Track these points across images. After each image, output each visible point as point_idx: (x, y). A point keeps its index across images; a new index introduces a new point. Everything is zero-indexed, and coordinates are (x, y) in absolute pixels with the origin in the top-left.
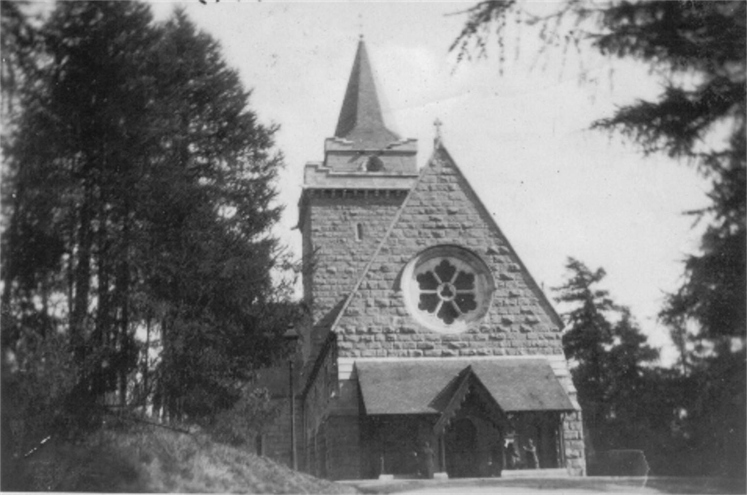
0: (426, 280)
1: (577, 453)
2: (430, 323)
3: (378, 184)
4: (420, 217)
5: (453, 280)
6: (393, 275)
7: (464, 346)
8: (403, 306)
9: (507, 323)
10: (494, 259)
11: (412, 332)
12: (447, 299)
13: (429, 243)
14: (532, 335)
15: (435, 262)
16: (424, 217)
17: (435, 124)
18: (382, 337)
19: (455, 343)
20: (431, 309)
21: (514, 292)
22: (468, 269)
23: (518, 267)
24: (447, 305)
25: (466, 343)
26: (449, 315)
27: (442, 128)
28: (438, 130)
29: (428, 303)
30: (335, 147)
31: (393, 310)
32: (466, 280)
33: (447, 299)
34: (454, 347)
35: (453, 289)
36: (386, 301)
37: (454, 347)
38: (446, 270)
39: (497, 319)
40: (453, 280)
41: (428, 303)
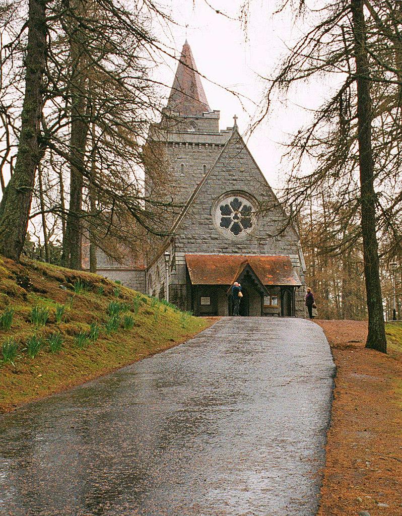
0: (225, 210)
2: (228, 233)
4: (223, 173)
11: (216, 239)
12: (236, 221)
15: (231, 199)
17: (234, 118)
19: (239, 246)
24: (236, 225)
26: (236, 230)
28: (235, 121)
29: (225, 223)
31: (207, 226)
34: (239, 248)
35: (239, 215)
37: (239, 248)
38: (236, 204)
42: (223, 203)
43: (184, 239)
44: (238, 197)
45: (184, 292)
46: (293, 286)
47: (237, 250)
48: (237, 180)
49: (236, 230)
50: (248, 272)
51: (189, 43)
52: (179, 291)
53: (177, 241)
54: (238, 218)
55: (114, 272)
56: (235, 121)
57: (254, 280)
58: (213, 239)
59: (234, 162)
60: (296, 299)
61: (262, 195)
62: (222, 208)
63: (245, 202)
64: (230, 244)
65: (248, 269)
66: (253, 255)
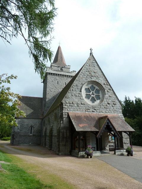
0: (87, 90)
1: (128, 143)
2: (88, 102)
3: (62, 73)
4: (86, 73)
7: (98, 110)
8: (82, 97)
9: (109, 104)
12: (93, 96)
13: (89, 80)
15: (90, 85)
16: (88, 73)
17: (90, 50)
18: (76, 105)
19: (95, 108)
20: (89, 98)
21: (110, 96)
22: (98, 88)
26: (93, 100)
27: (92, 51)
29: (88, 96)
30: (54, 65)
31: (79, 98)
33: (93, 96)
34: (95, 110)
36: (77, 95)
37: (95, 110)
39: (106, 103)
43: (67, 103)
44: (93, 85)
45: (68, 134)
47: (94, 111)
48: (93, 76)
49: (93, 100)
50: (108, 123)
51: (60, 46)
52: (65, 134)
54: (94, 95)
55: (30, 119)
57: (111, 128)
61: (104, 84)
63: (97, 87)
64: (91, 107)
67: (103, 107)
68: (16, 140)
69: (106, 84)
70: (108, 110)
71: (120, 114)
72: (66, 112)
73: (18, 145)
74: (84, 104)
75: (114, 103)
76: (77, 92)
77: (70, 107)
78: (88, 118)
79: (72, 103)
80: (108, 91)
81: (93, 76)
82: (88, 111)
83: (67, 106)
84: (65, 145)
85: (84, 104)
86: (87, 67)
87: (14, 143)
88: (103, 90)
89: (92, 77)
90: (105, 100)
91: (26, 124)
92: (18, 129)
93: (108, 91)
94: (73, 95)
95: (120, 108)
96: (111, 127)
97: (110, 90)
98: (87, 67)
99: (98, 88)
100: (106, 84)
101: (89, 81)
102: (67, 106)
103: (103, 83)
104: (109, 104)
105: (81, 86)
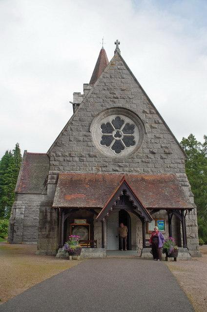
0: (106, 128)
1: (194, 236)
2: (108, 152)
4: (104, 92)
5: (122, 128)
6: (86, 123)
7: (126, 166)
8: (91, 141)
9: (153, 153)
10: (146, 116)
14: (168, 161)
15: (111, 118)
16: (107, 93)
18: (77, 159)
19: (120, 164)
20: (108, 145)
21: (157, 135)
22: (131, 122)
23: (160, 121)
24: (118, 142)
25: (127, 164)
26: (118, 148)
29: (106, 141)
30: (88, 87)
31: (85, 143)
32: (129, 128)
33: (118, 138)
34: (120, 166)
35: (122, 133)
36: (81, 138)
37: (120, 166)
38: (119, 122)
39: (147, 151)
40: (122, 128)
41: (106, 141)
42: (105, 121)
43: (59, 156)
46: (183, 210)
47: (118, 168)
48: (117, 98)
49: (118, 148)
50: (124, 191)
51: (105, 48)
52: (49, 214)
53: (52, 158)
54: (120, 136)
56: (117, 48)
58: (90, 156)
59: (116, 82)
60: (187, 224)
61: (144, 112)
62: (103, 126)
63: (127, 120)
65: (125, 188)
66: (136, 171)
67: (139, 160)
68: (18, 233)
69: (148, 112)
70: (150, 165)
71: (178, 175)
72: (54, 174)
73: (21, 243)
74: (95, 156)
75: (166, 150)
76: (81, 133)
77: (65, 164)
78: (94, 182)
79: (70, 154)
80: (152, 127)
81: (117, 98)
82: (104, 169)
83: (58, 161)
84: (48, 237)
85: (95, 156)
86: (105, 80)
87: (14, 240)
88: (141, 123)
89: (115, 100)
90: (145, 146)
91: (35, 204)
92: (21, 214)
93: (152, 127)
94: (72, 139)
95: (180, 161)
96: (132, 198)
97: (159, 123)
98: (105, 80)
99: (131, 122)
100: (148, 112)
101: (108, 109)
102: (58, 161)
103: (141, 111)
104: (153, 153)
105: (89, 120)
